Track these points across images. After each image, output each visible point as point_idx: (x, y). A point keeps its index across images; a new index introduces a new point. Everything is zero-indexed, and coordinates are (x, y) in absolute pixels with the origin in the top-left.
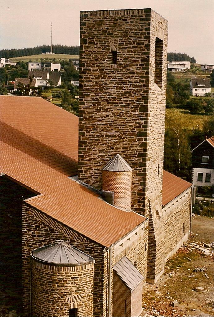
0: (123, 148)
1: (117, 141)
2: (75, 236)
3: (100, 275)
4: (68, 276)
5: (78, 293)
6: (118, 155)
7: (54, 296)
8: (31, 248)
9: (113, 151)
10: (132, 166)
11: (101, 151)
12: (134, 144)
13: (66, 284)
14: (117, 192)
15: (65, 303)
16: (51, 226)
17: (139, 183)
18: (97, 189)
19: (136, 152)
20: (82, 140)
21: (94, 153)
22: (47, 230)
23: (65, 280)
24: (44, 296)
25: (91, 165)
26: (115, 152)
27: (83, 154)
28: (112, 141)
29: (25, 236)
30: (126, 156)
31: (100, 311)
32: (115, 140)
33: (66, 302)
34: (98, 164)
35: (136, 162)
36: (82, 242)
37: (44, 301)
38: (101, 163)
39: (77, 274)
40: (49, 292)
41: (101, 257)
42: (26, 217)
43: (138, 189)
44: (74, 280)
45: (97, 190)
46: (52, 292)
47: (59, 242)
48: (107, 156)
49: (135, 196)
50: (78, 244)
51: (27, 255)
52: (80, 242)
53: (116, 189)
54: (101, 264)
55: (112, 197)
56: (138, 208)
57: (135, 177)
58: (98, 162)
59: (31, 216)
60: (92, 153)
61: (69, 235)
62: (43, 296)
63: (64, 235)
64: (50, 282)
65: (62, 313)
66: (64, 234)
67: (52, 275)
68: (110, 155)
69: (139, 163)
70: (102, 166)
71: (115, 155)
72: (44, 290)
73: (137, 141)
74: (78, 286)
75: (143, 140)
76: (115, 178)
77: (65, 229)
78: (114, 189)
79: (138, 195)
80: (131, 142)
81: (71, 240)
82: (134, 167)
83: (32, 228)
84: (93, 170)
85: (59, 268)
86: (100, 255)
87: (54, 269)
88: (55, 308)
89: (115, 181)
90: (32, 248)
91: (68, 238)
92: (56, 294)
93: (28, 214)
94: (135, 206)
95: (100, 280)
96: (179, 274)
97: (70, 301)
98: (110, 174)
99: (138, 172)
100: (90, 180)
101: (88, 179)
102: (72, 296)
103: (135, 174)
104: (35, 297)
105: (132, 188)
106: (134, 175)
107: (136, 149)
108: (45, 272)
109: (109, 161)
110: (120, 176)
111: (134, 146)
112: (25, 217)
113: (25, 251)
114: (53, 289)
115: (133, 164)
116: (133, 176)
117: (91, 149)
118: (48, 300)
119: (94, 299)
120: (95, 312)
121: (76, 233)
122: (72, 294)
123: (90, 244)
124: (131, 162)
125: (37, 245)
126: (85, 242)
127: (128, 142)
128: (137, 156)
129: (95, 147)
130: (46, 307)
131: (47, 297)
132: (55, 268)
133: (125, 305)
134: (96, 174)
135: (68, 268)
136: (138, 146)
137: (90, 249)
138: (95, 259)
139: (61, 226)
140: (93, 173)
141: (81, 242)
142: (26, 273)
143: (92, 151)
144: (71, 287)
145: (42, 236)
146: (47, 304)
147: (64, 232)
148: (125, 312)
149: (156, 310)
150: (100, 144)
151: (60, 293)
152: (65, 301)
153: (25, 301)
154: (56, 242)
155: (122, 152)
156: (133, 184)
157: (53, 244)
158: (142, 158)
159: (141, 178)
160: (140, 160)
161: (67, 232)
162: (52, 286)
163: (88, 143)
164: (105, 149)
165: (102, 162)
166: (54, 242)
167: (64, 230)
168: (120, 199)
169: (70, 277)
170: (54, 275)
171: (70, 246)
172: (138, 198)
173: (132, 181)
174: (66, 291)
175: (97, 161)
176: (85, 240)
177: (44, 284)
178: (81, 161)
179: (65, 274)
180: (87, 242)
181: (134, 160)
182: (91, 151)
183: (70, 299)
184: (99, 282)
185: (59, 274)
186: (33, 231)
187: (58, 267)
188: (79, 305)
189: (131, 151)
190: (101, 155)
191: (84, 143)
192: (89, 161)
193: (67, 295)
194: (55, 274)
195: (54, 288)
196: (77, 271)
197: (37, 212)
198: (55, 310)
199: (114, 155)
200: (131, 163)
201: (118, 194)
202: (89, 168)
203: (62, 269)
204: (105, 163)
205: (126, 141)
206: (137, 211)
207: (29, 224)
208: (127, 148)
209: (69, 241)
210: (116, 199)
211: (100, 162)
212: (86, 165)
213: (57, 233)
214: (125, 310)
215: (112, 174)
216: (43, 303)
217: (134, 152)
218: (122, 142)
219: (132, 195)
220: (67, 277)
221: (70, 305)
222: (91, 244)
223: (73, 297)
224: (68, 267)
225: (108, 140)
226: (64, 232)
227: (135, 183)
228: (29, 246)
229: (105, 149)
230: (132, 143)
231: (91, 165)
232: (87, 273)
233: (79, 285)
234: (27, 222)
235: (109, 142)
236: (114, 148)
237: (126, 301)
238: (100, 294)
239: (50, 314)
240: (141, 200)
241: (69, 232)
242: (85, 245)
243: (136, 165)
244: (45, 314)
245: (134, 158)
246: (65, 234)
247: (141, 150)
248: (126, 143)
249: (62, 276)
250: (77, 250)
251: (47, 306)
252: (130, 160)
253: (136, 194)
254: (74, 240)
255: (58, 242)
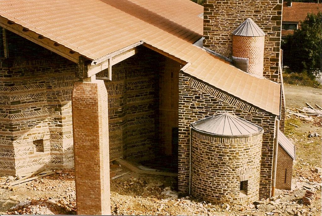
0: (255, 12)
1: (248, 4)
2: (241, 106)
3: (269, 145)
4: (240, 148)
5: (249, 165)
6: (249, 18)
7: (225, 169)
8: (189, 121)
9: (243, 15)
10: (264, 30)
11: (229, 15)
12: (267, 6)
13: (238, 157)
14: (252, 59)
15: (237, 176)
16: (214, 97)
17: (273, 49)
18: (225, 56)
19: (269, 15)
20: (208, 3)
21: (222, 17)
22: (209, 101)
23: (237, 152)
24: (213, 171)
25: (218, 31)
26: (245, 15)
27: (209, 19)
28: (242, 4)
29: (182, 109)
30: (258, 20)
31: (267, 181)
32: (246, 2)
33: (237, 175)
34: (226, 29)
35: (270, 26)
36: (249, 111)
37: (212, 176)
38: (229, 28)
39: (249, 145)
40: (219, 166)
41: (270, 126)
42: (184, 88)
43: (271, 55)
44: (247, 152)
45: (224, 57)
46: (223, 166)
47: (223, 113)
48: (237, 20)
49: (267, 62)
50: (245, 114)
51: (184, 129)
52: (247, 111)
53: (251, 55)
54: (271, 133)
55: (246, 64)
56: (270, 74)
57: (267, 42)
58: (226, 27)
59: (189, 87)
60: (220, 18)
61: (234, 105)
62: (211, 170)
63: (229, 105)
64: (220, 155)
65: (233, 186)
66: (229, 104)
67: (224, 148)
68: (240, 19)
69: (273, 27)
70: (231, 31)
71: (245, 19)
72: (213, 164)
73: (270, 3)
74: (250, 157)
75: (278, 2)
76: (250, 44)
77: (230, 98)
78: (249, 55)
79: (270, 61)
80: (265, 4)
81: (236, 111)
82: (267, 32)
83: (190, 100)
84: (221, 36)
85: (231, 140)
86: (270, 125)
87: (226, 141)
88: (226, 182)
89: (250, 47)
90: (190, 121)
91: (234, 108)
92: (228, 167)
93: (186, 84)
94: (267, 72)
95: (269, 150)
96: (298, 140)
97: (241, 174)
98: (244, 39)
99: (271, 37)
100: (217, 46)
101: (215, 45)
102: (244, 168)
103: (268, 39)
104: (200, 172)
105: (265, 53)
106: (267, 40)
107: (270, 12)
108: (214, 145)
109: (239, 25)
110: (253, 42)
111: (267, 9)
112: (182, 88)
113: (182, 125)
114: (224, 162)
115: (265, 29)
116: (266, 41)
117: (218, 13)
118: (217, 174)
119: (261, 169)
120: (262, 183)
121: (242, 102)
122: (243, 166)
123: (259, 113)
124: (264, 26)
125: (197, 118)
126: (253, 111)
127: (261, 5)
128: (270, 19)
129: (223, 11)
130: (215, 181)
131: (216, 171)
132: (227, 140)
133: (286, 174)
134: (224, 40)
135: (241, 140)
136: (272, 9)
137: (258, 118)
138: (264, 129)
139: (225, 95)
140: (221, 39)
141: (248, 112)
142: (183, 148)
143: (220, 15)
144: (243, 160)
145: (203, 108)
146: (216, 178)
147: (229, 102)
148: (285, 181)
149: (303, 178)
150: (229, 8)
151: (232, 166)
152: (236, 174)
153: (181, 177)
154: (219, 113)
155: (253, 15)
156: (265, 49)
157: (215, 116)
158: (277, 22)
159: (274, 43)
160: (273, 24)
161: (233, 102)
162: (222, 159)
163: (214, 7)
164: (234, 13)
165: (230, 27)
166: (217, 113)
167: (228, 100)
168: (255, 65)
169: (243, 149)
170: (225, 148)
171: (235, 116)
172: (271, 64)
173: (265, 47)
174: (238, 164)
175: (226, 26)
176: (253, 110)
177: (213, 157)
178: (206, 26)
179: (238, 146)
180: (255, 111)
181: (267, 24)
182: (218, 16)
183: (242, 171)
184: (267, 152)
185: (231, 146)
186: (192, 102)
187: (230, 139)
188: (250, 177)
189: (264, 14)
190: (230, 20)
191: (211, 7)
192: (216, 26)
193: (239, 167)
194: (226, 147)
195: (225, 162)
196: (249, 142)
197: (197, 82)
198: (225, 184)
199: (244, 19)
200: (263, 27)
201: (253, 60)
202: (215, 33)
203: (234, 141)
204: (234, 28)
205: (258, 4)
206: (269, 78)
207: (187, 95)
208: (259, 11)
209: (234, 111)
210: (251, 66)
211: (228, 27)
212: (212, 31)
213: (221, 103)
214: (285, 179)
215: (246, 40)
216: (212, 178)
217: (267, 15)
218: (254, 4)
219: (264, 61)
220: (240, 149)
221: (241, 178)
222: (260, 113)
223: (245, 169)
224: (241, 139)
225: (238, 2)
226: (229, 102)
227: (268, 49)
228: (186, 119)
229: (235, 13)
230: (265, 6)
231: (218, 31)
232: (258, 143)
233: (250, 157)
234: (186, 93)
235: (239, 5)
236: (244, 12)
237: (286, 169)
238: (268, 164)
239: (219, 188)
240: (274, 66)
241: (234, 102)
242: (252, 115)
243: (270, 29)
244: (213, 188)
245: (268, 21)
246: (230, 104)
247: (275, 12)
248: (259, 6)
249: (234, 148)
250: (244, 120)
251: (215, 180)
252: (263, 24)
253: (269, 60)
254: (241, 109)
255: (221, 113)
